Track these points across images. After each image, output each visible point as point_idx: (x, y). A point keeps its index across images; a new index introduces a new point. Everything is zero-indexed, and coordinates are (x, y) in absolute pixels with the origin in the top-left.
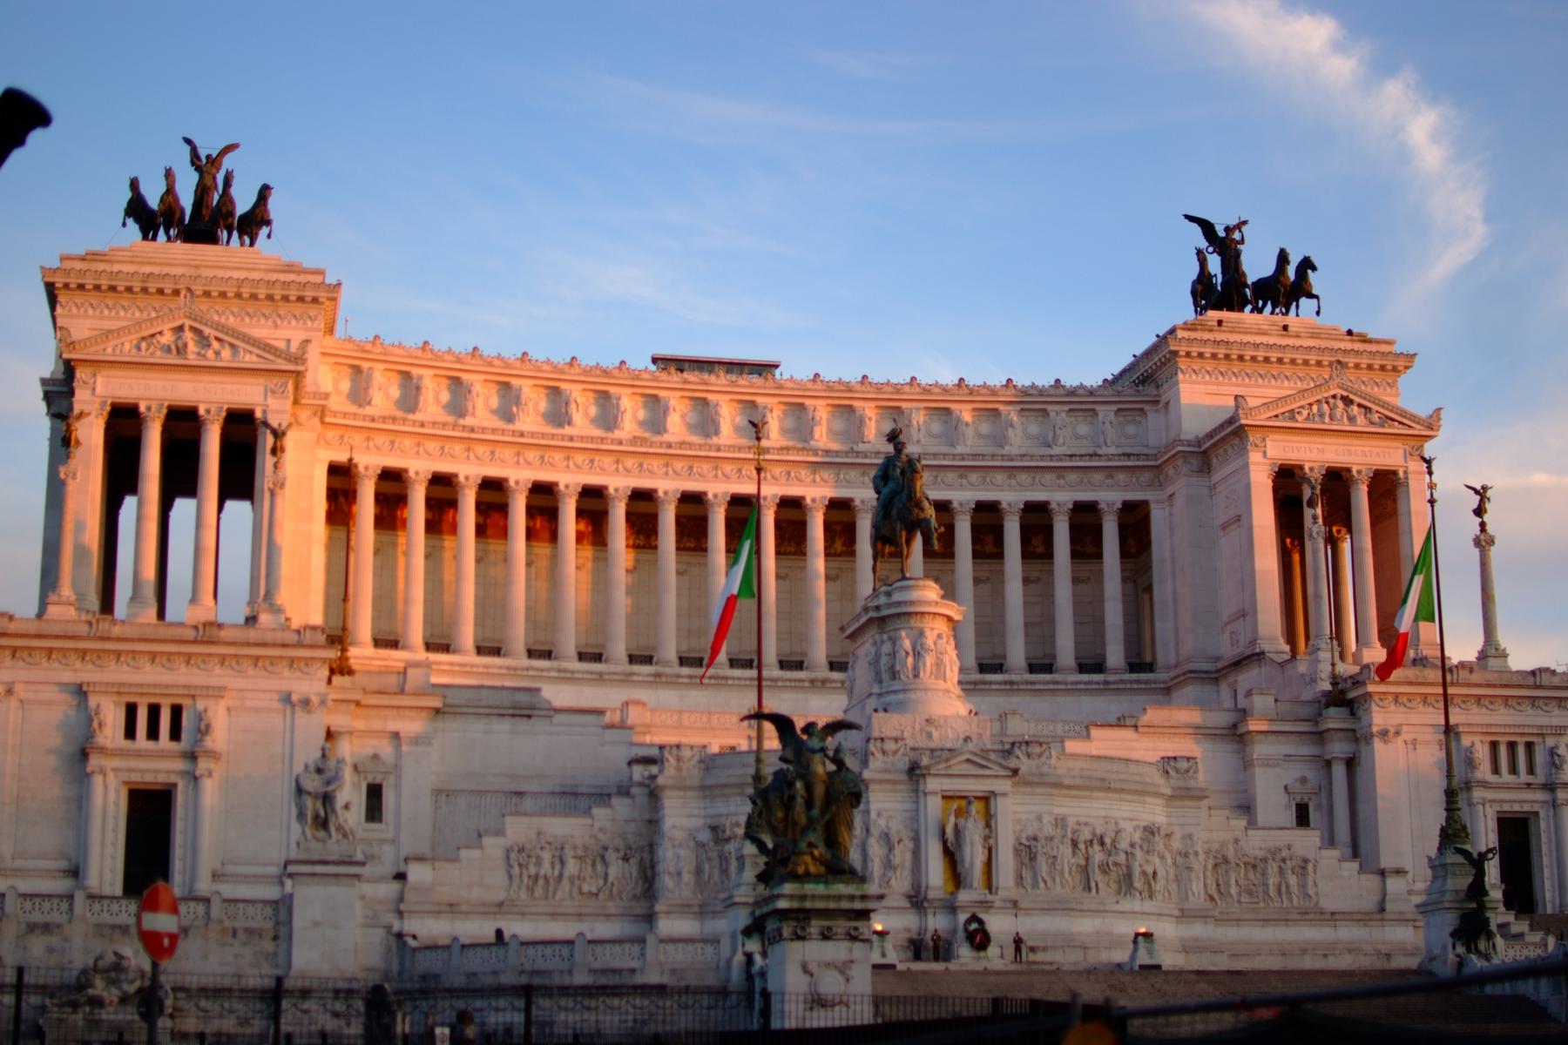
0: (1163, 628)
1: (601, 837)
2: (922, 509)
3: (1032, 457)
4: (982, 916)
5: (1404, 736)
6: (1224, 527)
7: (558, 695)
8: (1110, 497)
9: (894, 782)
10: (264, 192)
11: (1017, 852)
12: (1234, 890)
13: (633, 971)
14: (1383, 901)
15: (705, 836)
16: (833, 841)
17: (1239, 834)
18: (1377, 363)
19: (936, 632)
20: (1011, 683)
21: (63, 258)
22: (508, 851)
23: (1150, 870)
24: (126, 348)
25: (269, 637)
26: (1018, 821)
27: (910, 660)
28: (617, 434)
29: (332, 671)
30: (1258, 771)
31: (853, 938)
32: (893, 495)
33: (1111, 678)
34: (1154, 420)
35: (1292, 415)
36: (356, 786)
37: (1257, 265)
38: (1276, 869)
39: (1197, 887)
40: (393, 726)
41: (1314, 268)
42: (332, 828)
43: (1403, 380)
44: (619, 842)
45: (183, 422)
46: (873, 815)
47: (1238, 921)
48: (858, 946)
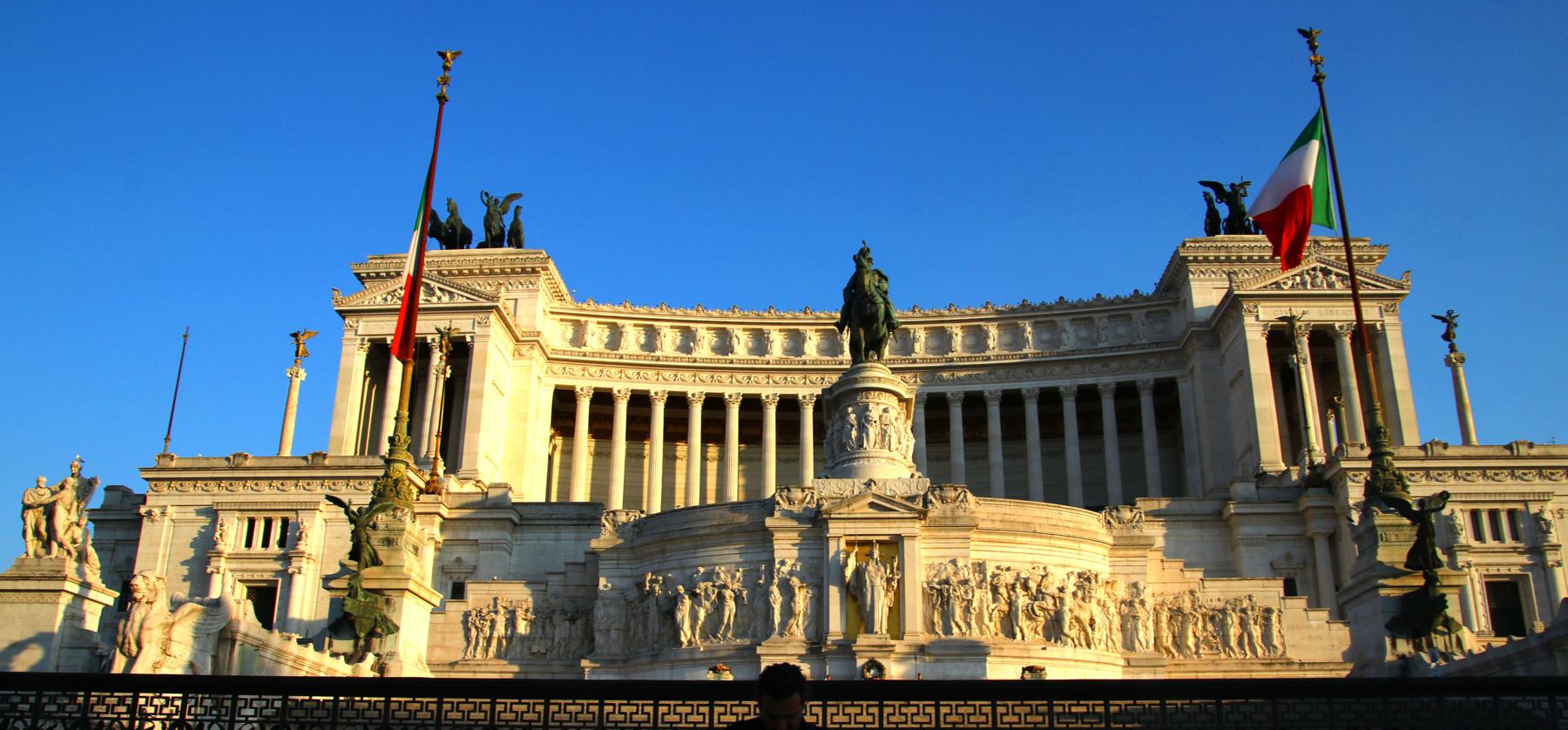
0: (1192, 473)
1: (552, 600)
2: (875, 304)
4: (883, 662)
6: (1232, 384)
8: (1145, 377)
11: (927, 596)
12: (1191, 642)
15: (633, 594)
19: (882, 407)
22: (467, 615)
26: (931, 566)
27: (854, 433)
28: (767, 357)
29: (421, 491)
30: (1243, 550)
38: (1236, 620)
39: (1145, 635)
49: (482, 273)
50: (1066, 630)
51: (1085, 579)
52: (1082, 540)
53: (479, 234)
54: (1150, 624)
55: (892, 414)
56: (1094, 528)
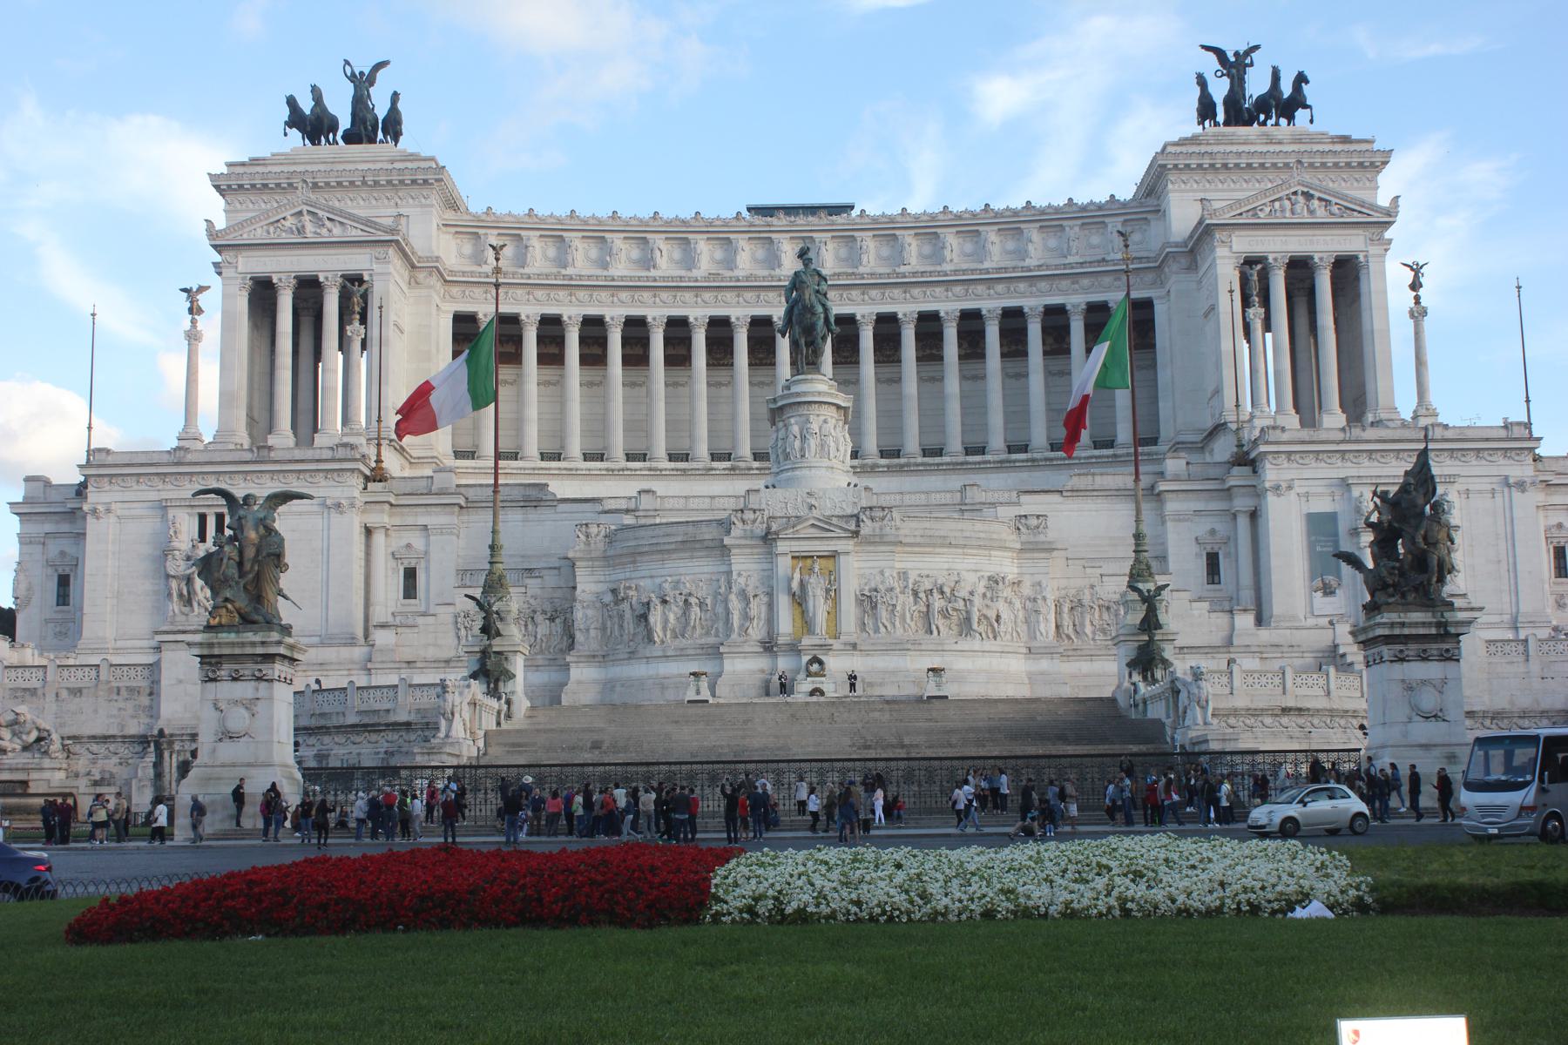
0: (1164, 407)
2: (814, 314)
3: (1048, 267)
5: (1297, 489)
6: (1206, 315)
7: (561, 488)
9: (752, 547)
10: (395, 97)
11: (860, 602)
13: (388, 711)
14: (1230, 638)
15: (608, 598)
16: (258, 598)
17: (1095, 581)
18: (1355, 160)
20: (1033, 460)
21: (230, 165)
23: (992, 614)
24: (259, 234)
25: (327, 454)
26: (862, 576)
27: (797, 444)
29: (367, 479)
30: (1169, 524)
31: (259, 679)
32: (796, 302)
33: (1119, 452)
34: (1155, 227)
35: (1254, 211)
36: (396, 570)
37: (1257, 84)
40: (422, 520)
41: (1307, 82)
42: (195, 605)
43: (1380, 178)
44: (548, 608)
45: (309, 288)
46: (735, 576)
47: (1091, 657)
48: (263, 685)
49: (364, 183)
50: (975, 626)
51: (994, 581)
52: (992, 548)
53: (345, 123)
54: (1052, 617)
55: (832, 422)
56: (1004, 536)
